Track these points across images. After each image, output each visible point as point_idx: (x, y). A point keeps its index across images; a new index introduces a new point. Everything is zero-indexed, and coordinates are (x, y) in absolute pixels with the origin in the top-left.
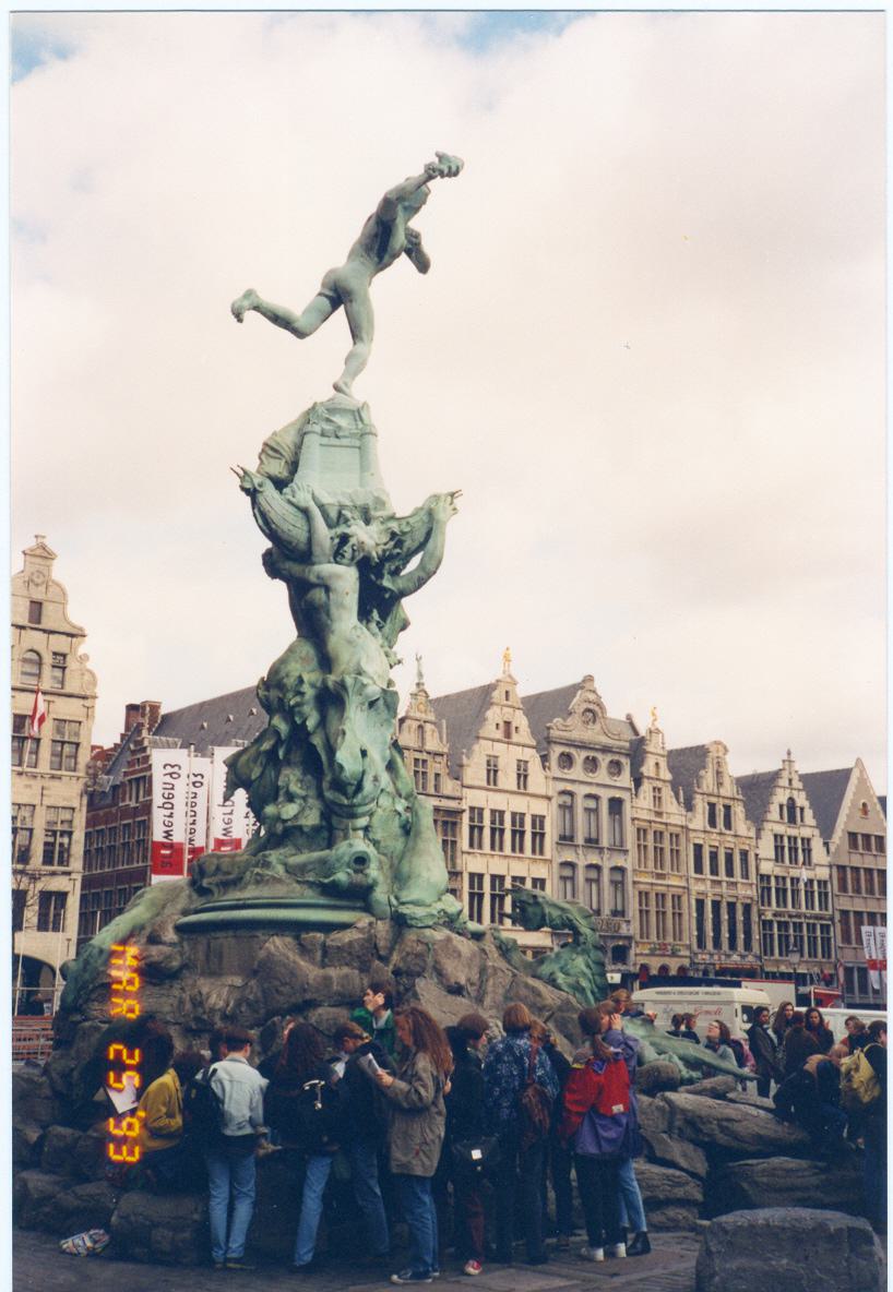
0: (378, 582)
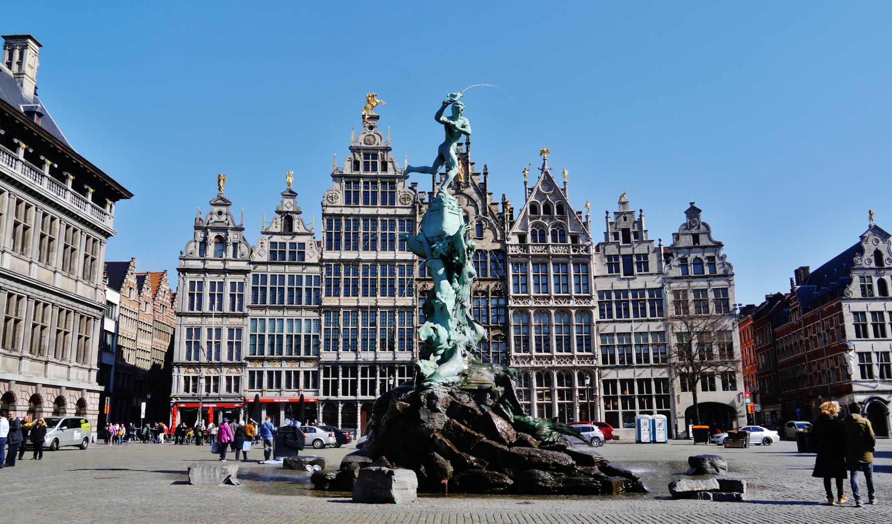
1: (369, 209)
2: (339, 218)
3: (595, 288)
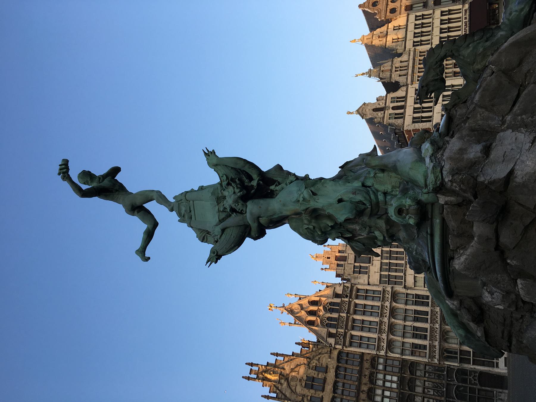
0: (255, 188)
3: (378, 285)
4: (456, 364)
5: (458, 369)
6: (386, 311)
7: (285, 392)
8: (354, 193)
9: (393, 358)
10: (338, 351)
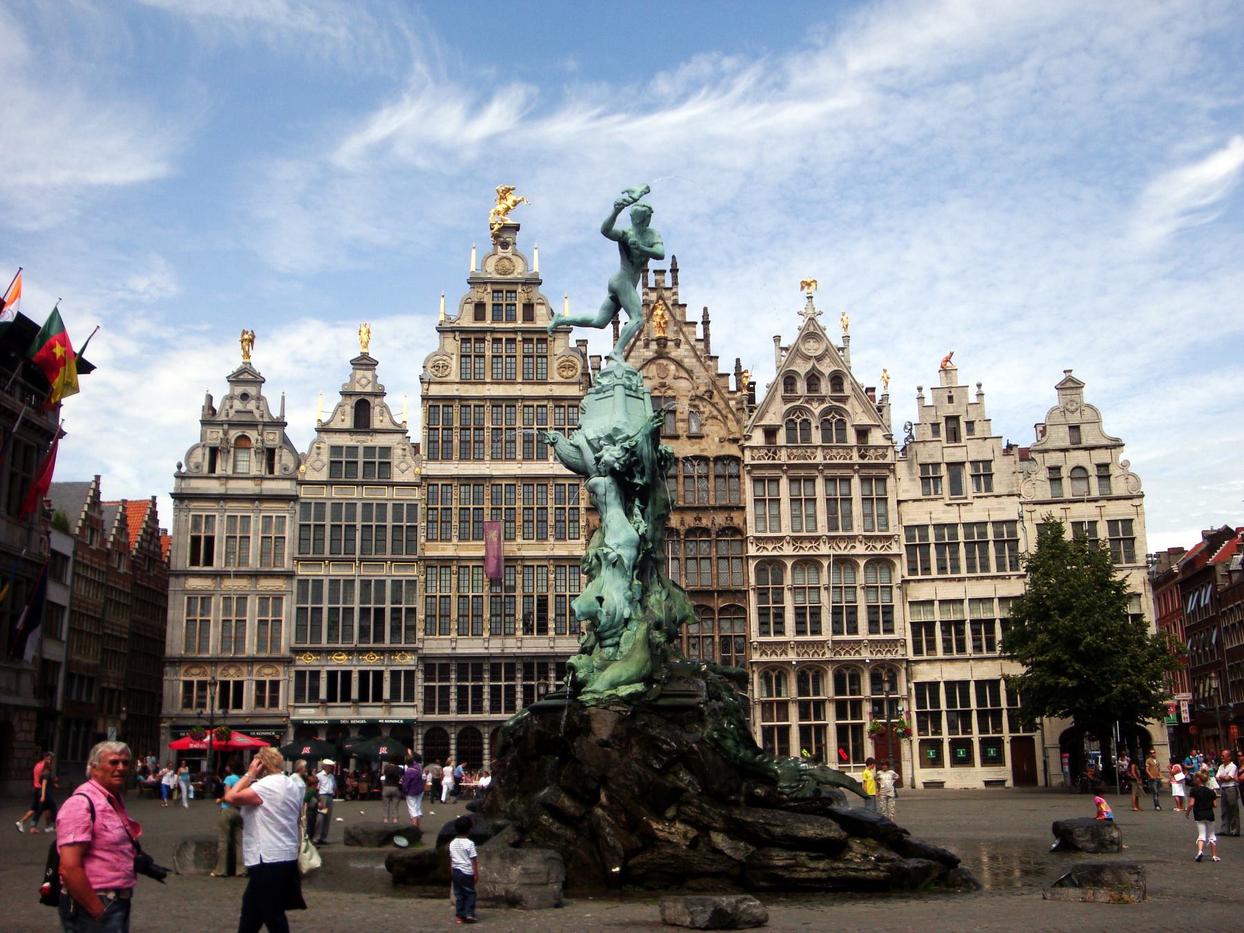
1: (501, 387)
2: (450, 403)
4: (756, 696)
5: (747, 699)
6: (843, 546)
7: (633, 358)
8: (608, 614)
9: (745, 571)
10: (739, 454)
